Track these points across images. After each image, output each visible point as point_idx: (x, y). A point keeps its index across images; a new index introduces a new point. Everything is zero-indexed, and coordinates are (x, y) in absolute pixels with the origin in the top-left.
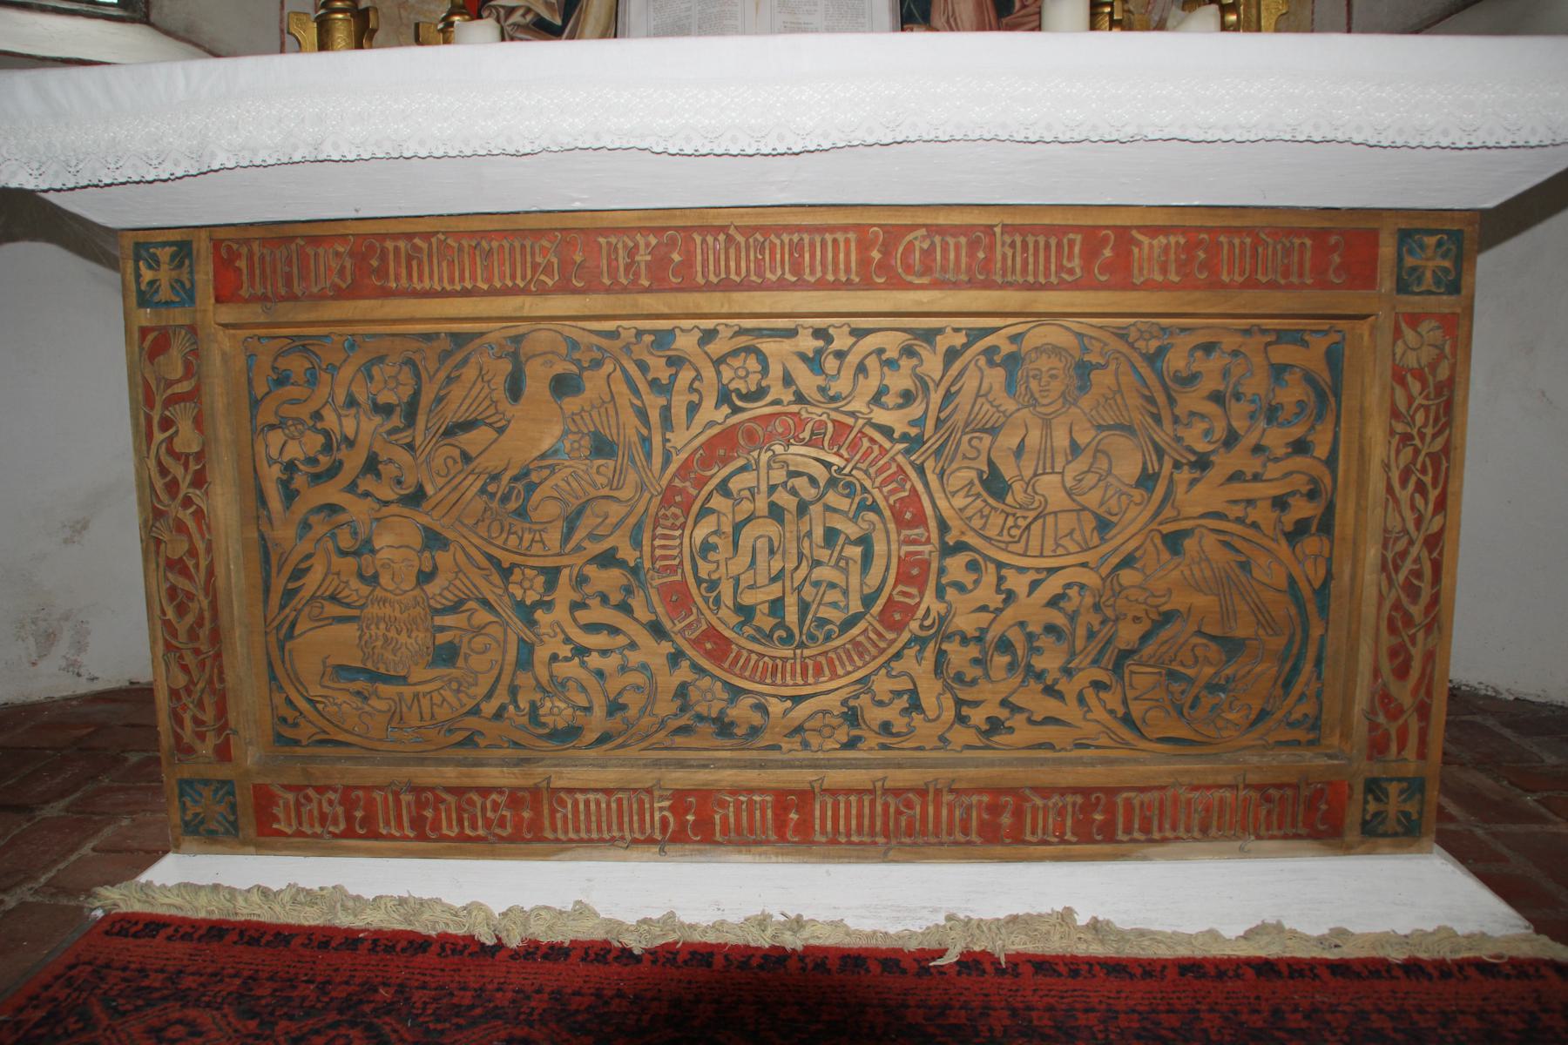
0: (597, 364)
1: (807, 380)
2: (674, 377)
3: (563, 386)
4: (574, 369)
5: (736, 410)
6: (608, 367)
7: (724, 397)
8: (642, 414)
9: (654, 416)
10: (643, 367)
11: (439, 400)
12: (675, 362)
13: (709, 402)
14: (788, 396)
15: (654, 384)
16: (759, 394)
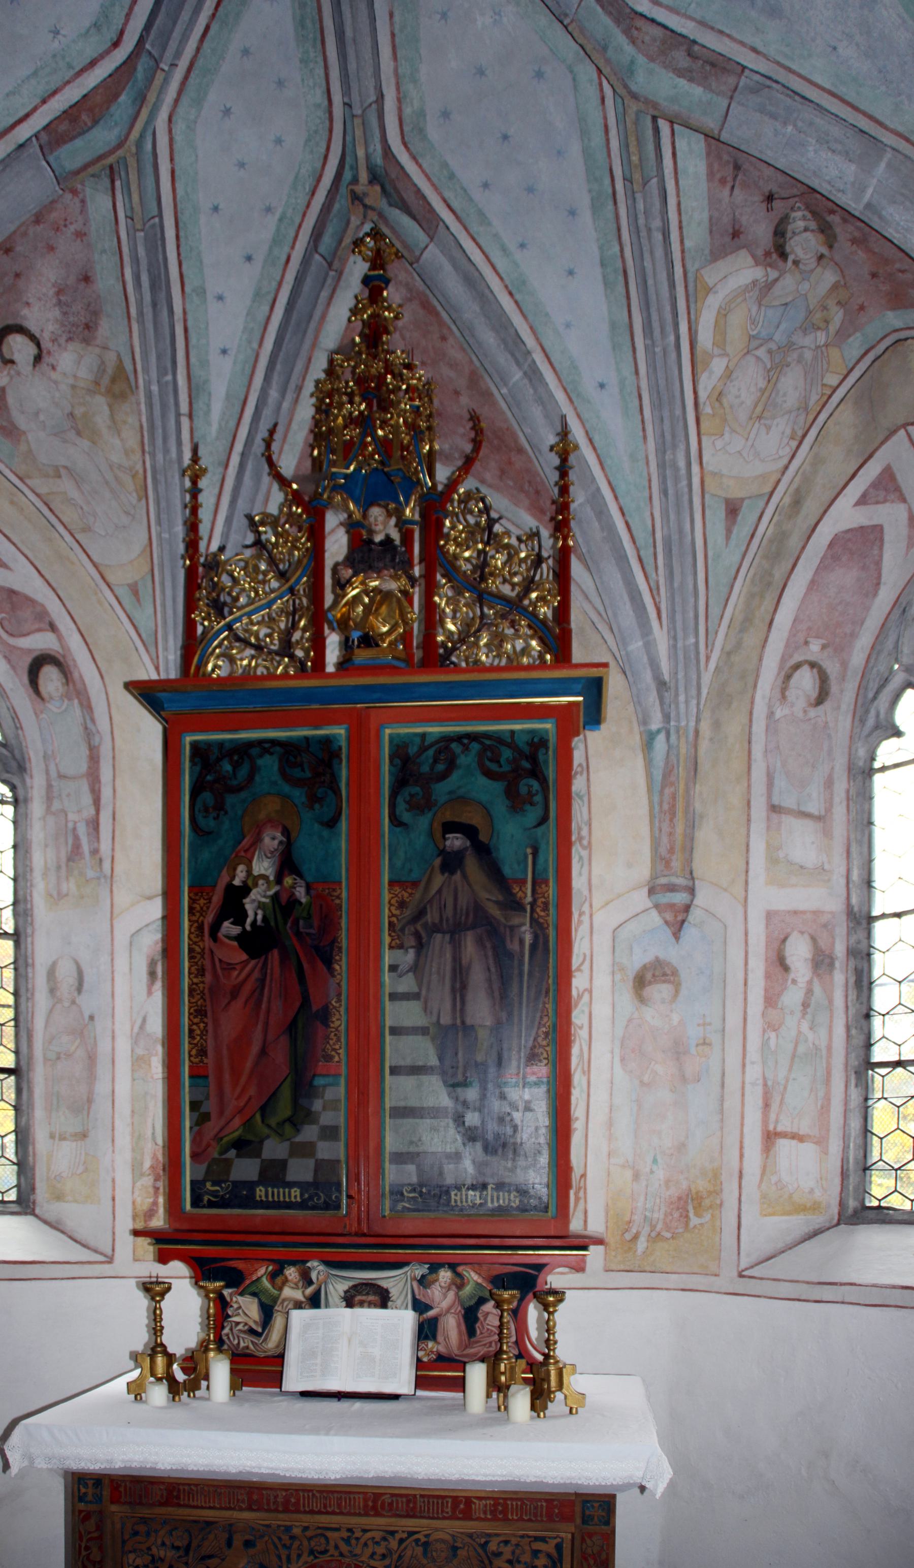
0: (262, 1536)
1: (344, 1548)
2: (291, 1545)
3: (248, 1544)
4: (252, 1538)
5: (316, 1557)
6: (266, 1538)
7: (311, 1552)
8: (279, 1557)
9: (284, 1557)
10: (280, 1539)
11: (199, 1546)
12: (293, 1538)
13: (306, 1554)
14: (336, 1554)
15: (284, 1546)
16: (325, 1552)
